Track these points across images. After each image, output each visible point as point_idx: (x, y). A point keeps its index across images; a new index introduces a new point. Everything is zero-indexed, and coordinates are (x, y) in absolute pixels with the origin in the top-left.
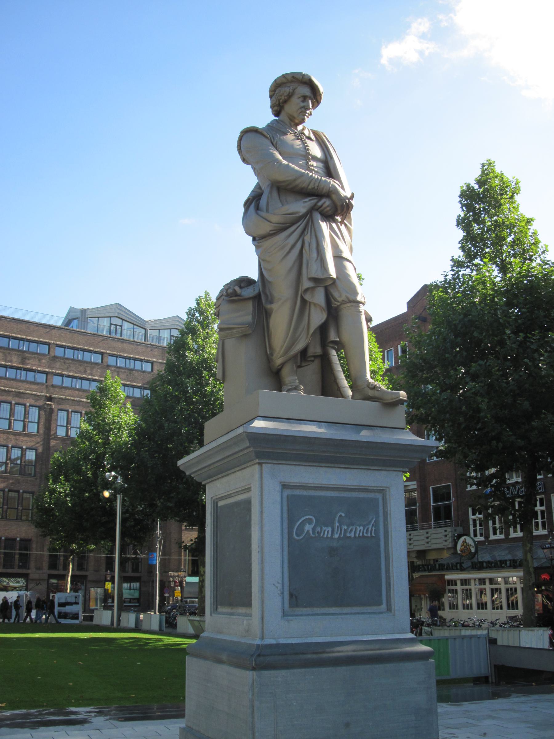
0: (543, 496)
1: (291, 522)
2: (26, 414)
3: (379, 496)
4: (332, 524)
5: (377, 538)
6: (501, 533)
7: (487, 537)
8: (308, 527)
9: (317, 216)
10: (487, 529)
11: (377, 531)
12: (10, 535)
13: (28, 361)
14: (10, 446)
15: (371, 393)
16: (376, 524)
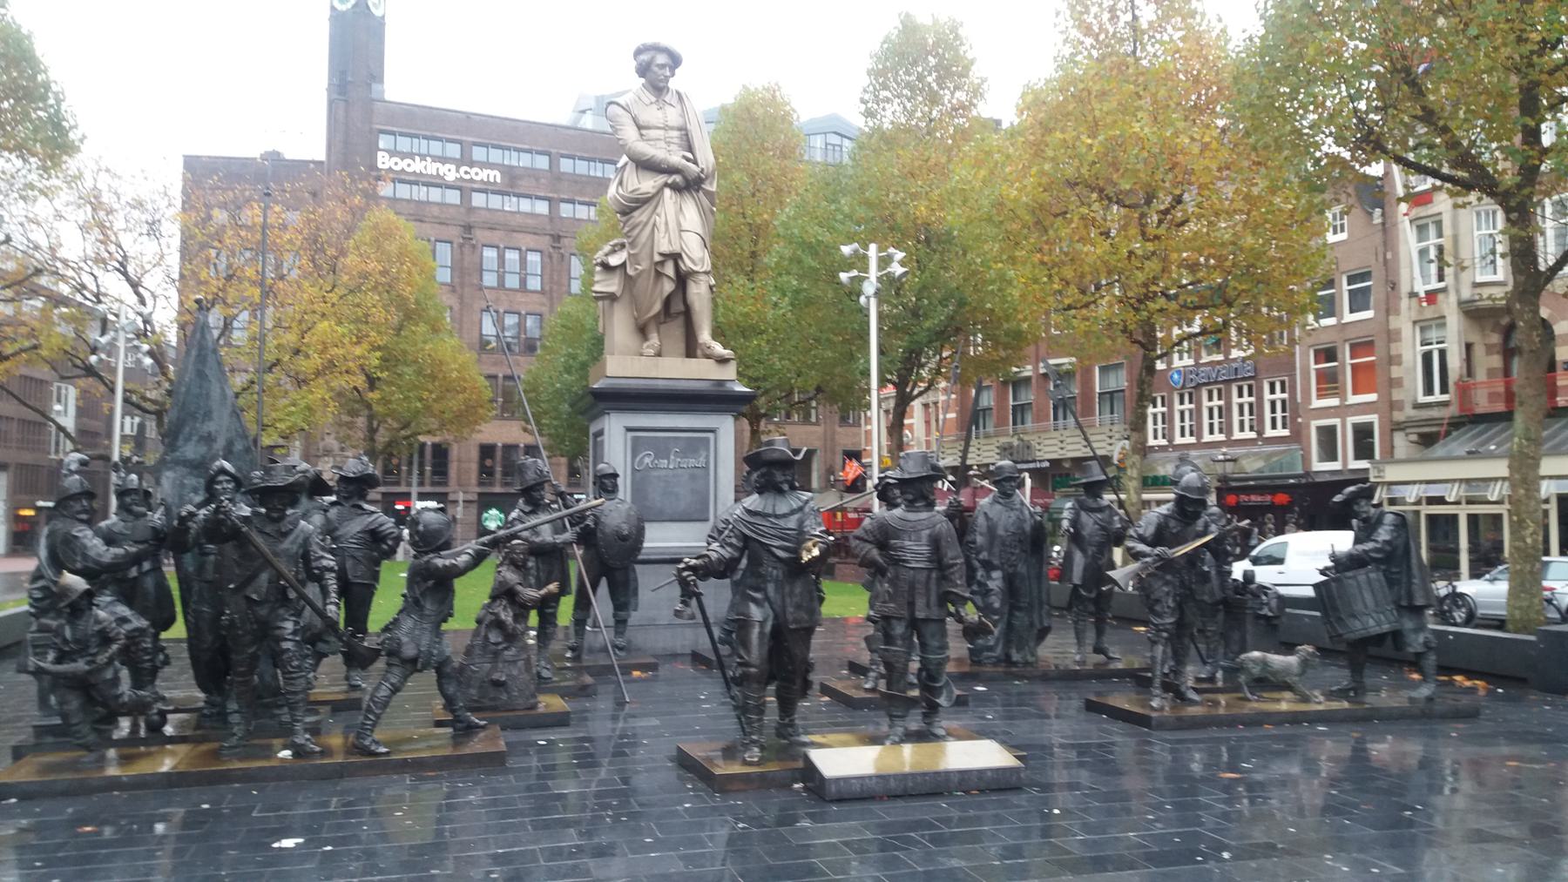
0: (1221, 386)
1: (634, 456)
2: (523, 262)
3: (710, 435)
4: (668, 459)
5: (706, 468)
6: (1191, 435)
7: (1170, 441)
8: (647, 460)
9: (667, 192)
10: (1172, 428)
11: (707, 463)
12: (510, 441)
13: (520, 183)
14: (501, 311)
15: (708, 352)
16: (707, 457)
